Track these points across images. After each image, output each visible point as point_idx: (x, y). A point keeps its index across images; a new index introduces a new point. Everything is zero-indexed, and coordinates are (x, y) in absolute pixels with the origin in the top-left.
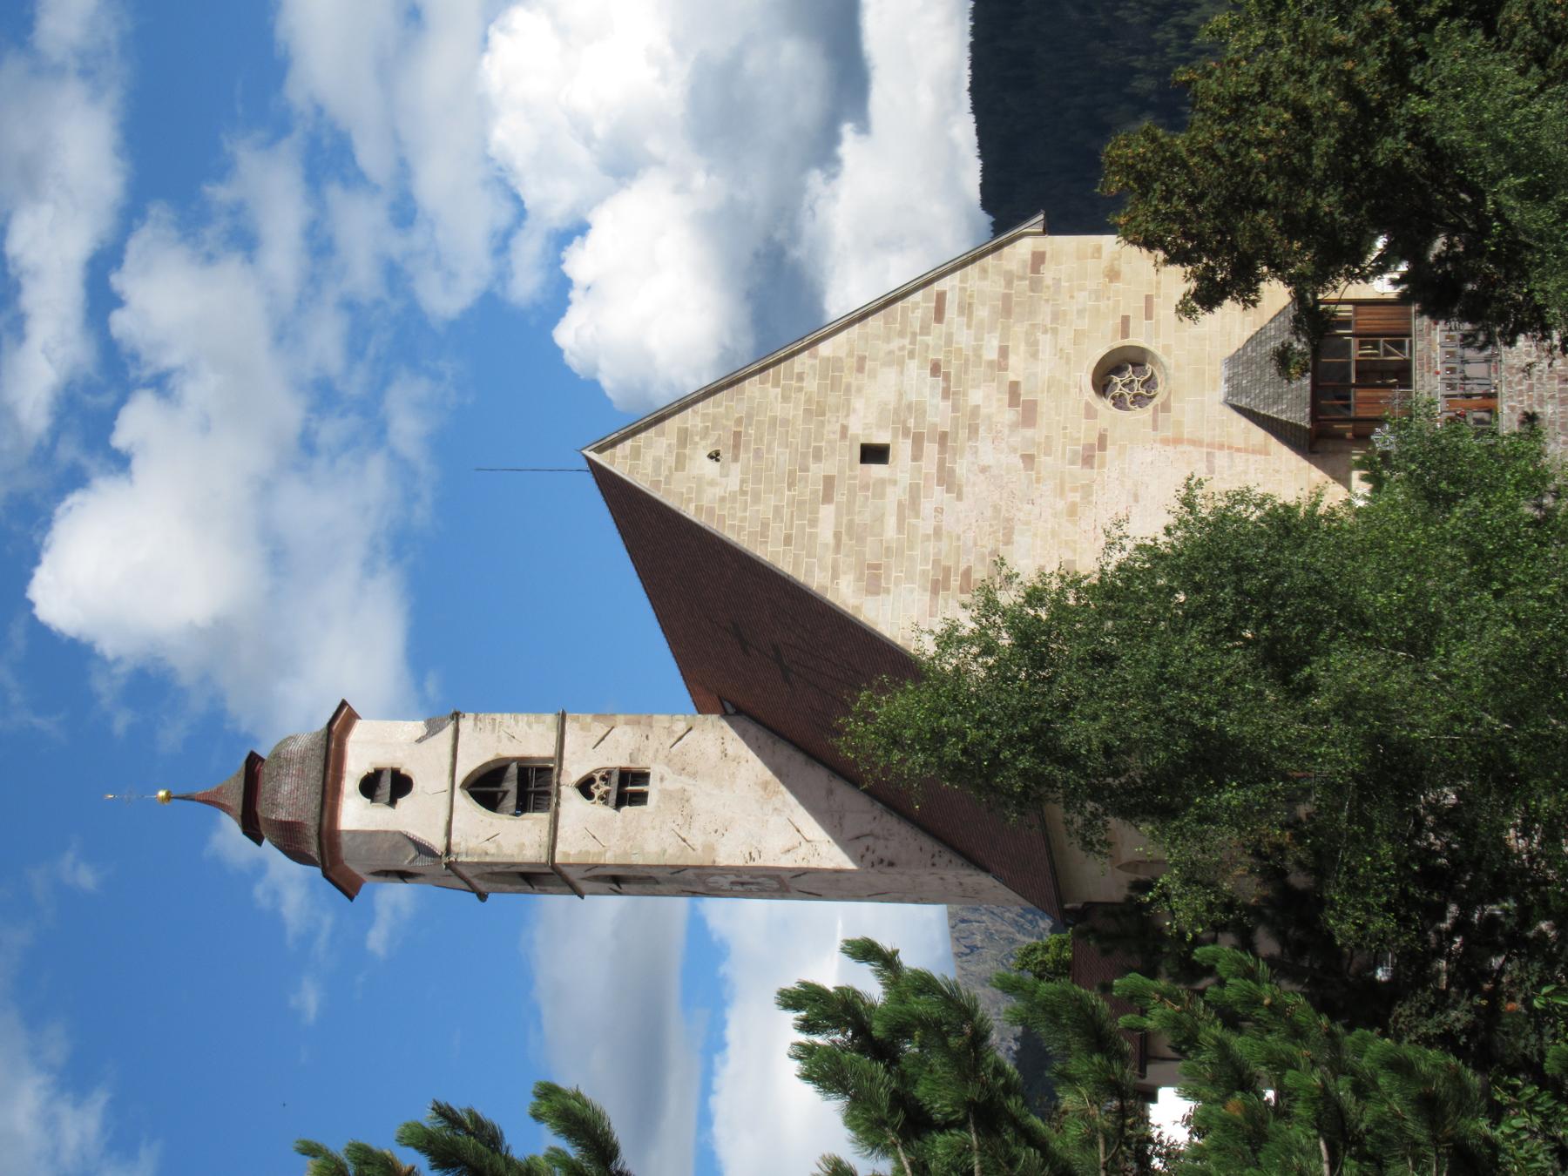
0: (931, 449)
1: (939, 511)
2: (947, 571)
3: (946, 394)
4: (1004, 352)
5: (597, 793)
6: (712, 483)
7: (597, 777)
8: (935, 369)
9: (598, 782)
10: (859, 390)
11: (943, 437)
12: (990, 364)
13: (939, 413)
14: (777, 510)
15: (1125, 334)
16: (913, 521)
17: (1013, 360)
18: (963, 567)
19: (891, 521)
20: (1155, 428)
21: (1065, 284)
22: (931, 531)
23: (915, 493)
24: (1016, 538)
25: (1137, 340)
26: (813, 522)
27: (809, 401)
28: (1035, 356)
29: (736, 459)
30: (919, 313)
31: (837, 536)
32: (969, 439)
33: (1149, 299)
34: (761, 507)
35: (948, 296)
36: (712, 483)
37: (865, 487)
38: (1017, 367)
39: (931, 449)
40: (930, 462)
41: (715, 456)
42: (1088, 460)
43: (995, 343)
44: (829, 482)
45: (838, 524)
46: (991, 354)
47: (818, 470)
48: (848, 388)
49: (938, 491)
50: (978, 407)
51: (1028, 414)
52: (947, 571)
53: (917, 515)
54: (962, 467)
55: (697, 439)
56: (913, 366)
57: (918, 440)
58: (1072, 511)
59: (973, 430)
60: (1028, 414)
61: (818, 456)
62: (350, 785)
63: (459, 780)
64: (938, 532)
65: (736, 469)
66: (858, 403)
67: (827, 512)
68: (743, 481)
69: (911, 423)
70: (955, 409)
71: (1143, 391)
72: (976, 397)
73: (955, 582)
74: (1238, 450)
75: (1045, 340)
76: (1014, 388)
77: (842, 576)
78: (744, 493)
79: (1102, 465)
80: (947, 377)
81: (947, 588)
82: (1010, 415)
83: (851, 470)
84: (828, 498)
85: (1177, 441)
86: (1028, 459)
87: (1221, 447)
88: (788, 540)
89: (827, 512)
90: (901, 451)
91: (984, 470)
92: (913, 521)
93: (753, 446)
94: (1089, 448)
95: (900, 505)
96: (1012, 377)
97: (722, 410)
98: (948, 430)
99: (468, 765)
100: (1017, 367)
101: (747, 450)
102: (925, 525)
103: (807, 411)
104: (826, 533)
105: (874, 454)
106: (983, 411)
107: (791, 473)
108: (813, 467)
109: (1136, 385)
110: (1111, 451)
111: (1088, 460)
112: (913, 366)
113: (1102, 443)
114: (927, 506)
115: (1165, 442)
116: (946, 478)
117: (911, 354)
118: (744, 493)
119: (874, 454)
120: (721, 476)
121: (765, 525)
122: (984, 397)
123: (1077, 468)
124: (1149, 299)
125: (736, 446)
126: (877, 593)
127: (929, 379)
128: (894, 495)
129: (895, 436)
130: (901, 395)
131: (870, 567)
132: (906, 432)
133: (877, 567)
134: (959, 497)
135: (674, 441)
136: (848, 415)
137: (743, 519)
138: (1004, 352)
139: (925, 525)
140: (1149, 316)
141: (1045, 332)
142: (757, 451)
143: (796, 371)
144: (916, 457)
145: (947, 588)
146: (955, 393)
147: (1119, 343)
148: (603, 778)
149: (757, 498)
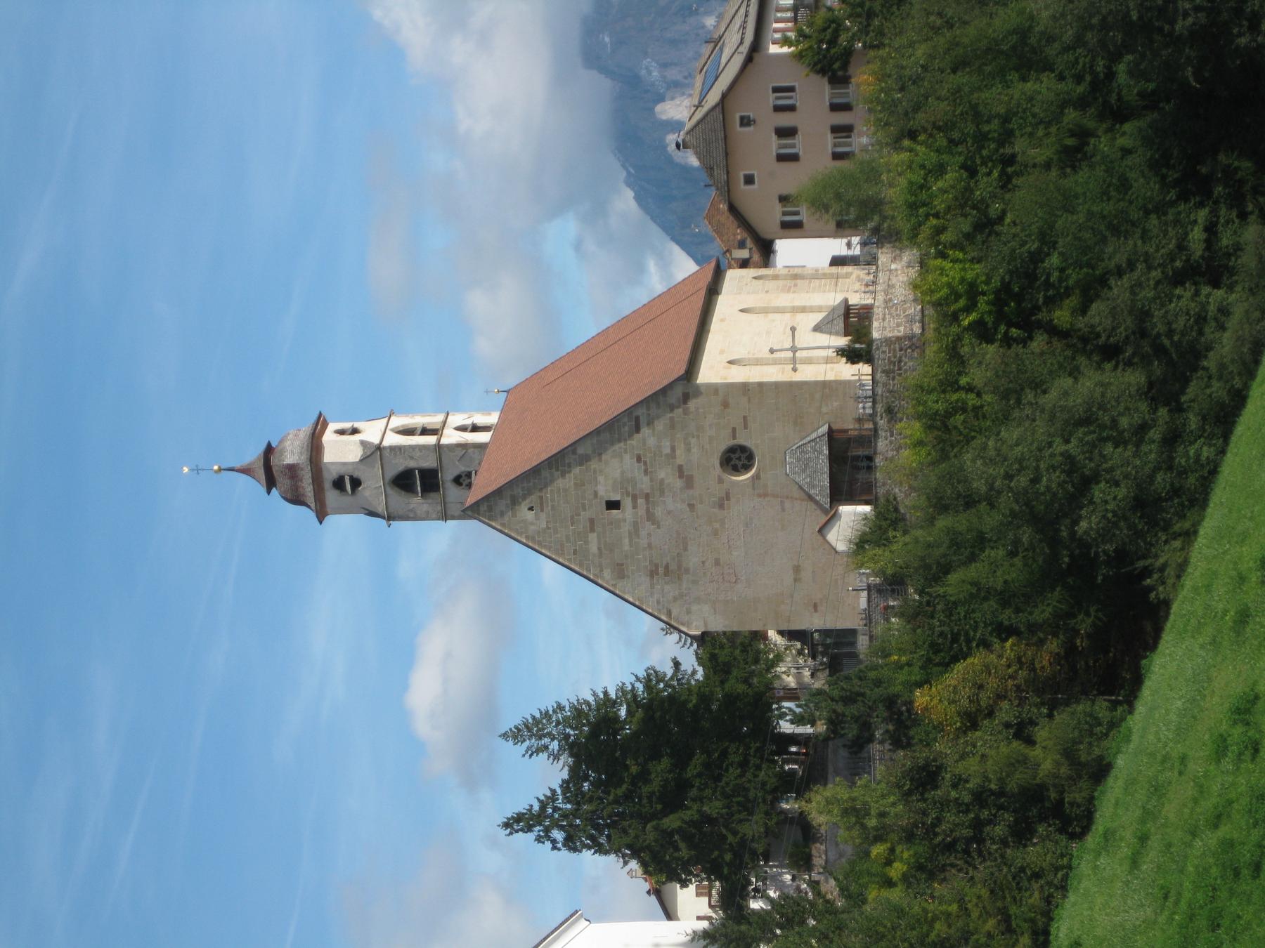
0: (641, 501)
1: (649, 535)
2: (657, 566)
3: (646, 472)
4: (673, 449)
5: (464, 484)
6: (532, 524)
7: (463, 475)
8: (639, 459)
9: (464, 478)
10: (601, 471)
11: (647, 496)
12: (667, 455)
13: (644, 484)
14: (567, 537)
15: (734, 437)
16: (637, 540)
17: (678, 452)
18: (664, 563)
19: (626, 541)
20: (754, 489)
21: (701, 410)
22: (646, 546)
23: (635, 524)
24: (689, 547)
25: (741, 441)
26: (586, 542)
27: (575, 478)
28: (689, 450)
29: (542, 510)
30: (626, 428)
31: (599, 549)
32: (661, 496)
33: (745, 418)
34: (559, 536)
35: (641, 418)
36: (532, 524)
37: (611, 523)
38: (681, 458)
39: (641, 501)
40: (641, 511)
41: (531, 509)
42: (721, 506)
43: (668, 444)
44: (592, 521)
45: (599, 543)
46: (667, 451)
47: (586, 515)
48: (595, 472)
49: (648, 524)
50: (662, 480)
51: (689, 482)
52: (657, 566)
53: (638, 537)
54: (659, 512)
55: (520, 500)
56: (627, 457)
57: (635, 498)
58: (716, 533)
59: (662, 493)
60: (689, 482)
61: (584, 509)
62: (328, 485)
63: (387, 481)
64: (650, 546)
65: (543, 516)
66: (601, 479)
67: (593, 537)
68: (547, 522)
69: (630, 489)
70: (651, 480)
71: (746, 462)
72: (662, 474)
73: (661, 570)
74: (796, 499)
75: (693, 441)
76: (680, 468)
77: (605, 571)
78: (549, 528)
79: (729, 508)
80: (645, 463)
81: (657, 574)
82: (679, 483)
83: (602, 514)
84: (592, 530)
85: (765, 495)
86: (691, 506)
87: (787, 498)
88: (575, 552)
89: (593, 537)
90: (627, 503)
91: (669, 513)
92: (637, 540)
93: (550, 504)
94: (721, 499)
95: (630, 533)
96: (679, 461)
97: (531, 484)
98: (649, 491)
99: (392, 472)
100: (681, 458)
101: (547, 506)
102: (644, 542)
103: (575, 484)
104: (594, 548)
105: (613, 505)
106: (666, 482)
107: (572, 518)
108: (582, 513)
109: (742, 459)
110: (733, 500)
111: (721, 506)
112: (627, 457)
113: (728, 497)
114: (643, 533)
115: (759, 496)
116: (650, 517)
117: (626, 452)
118: (549, 528)
119: (613, 505)
120: (536, 519)
121: (562, 545)
122: (665, 474)
123: (716, 510)
124: (745, 418)
125: (542, 504)
126: (623, 578)
127: (636, 464)
128: (626, 528)
129: (622, 495)
130: (623, 473)
131: (618, 564)
132: (628, 494)
133: (622, 565)
134: (659, 527)
135: (509, 502)
136: (596, 486)
137: (550, 542)
138: (673, 449)
139: (644, 542)
140: (746, 427)
141: (693, 437)
142: (553, 507)
143: (567, 462)
144: (635, 507)
145: (657, 574)
146: (651, 472)
147: (731, 442)
148: (466, 475)
149: (556, 532)
